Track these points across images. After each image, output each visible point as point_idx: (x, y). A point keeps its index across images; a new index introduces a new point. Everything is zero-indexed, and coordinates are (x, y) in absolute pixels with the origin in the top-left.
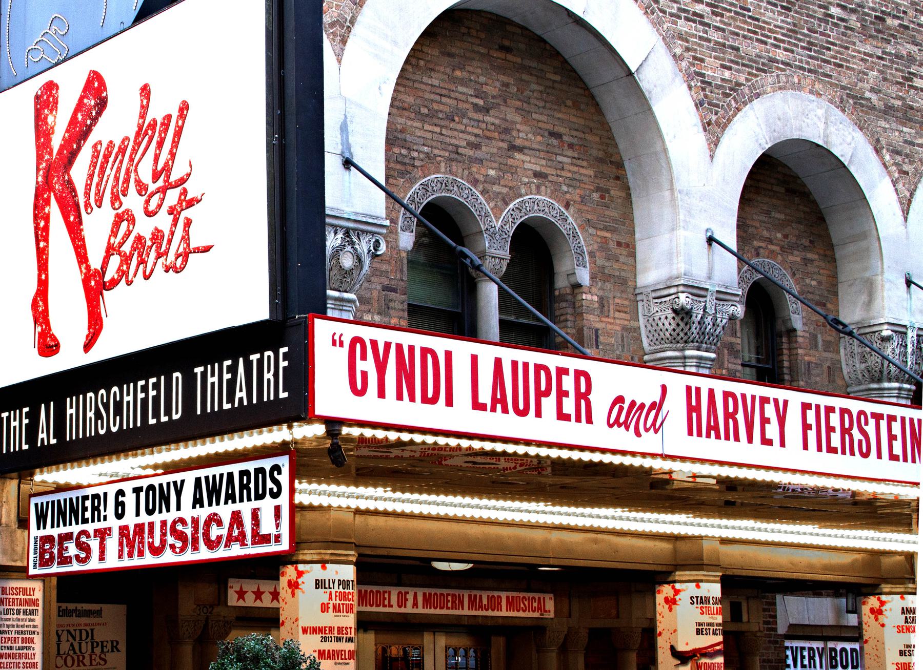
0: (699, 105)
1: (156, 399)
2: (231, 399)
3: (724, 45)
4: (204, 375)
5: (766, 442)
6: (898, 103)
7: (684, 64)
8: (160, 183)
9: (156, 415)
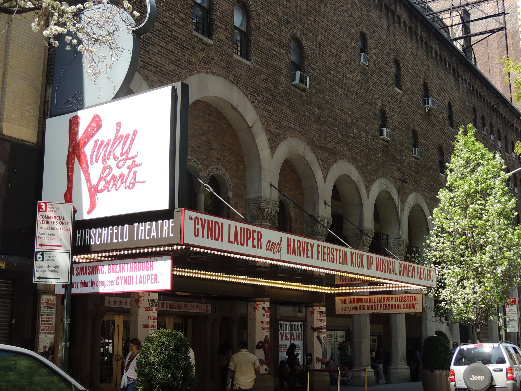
0: (269, 140)
1: (117, 234)
2: (149, 235)
4: (138, 227)
5: (308, 257)
6: (323, 145)
8: (124, 157)
9: (117, 238)
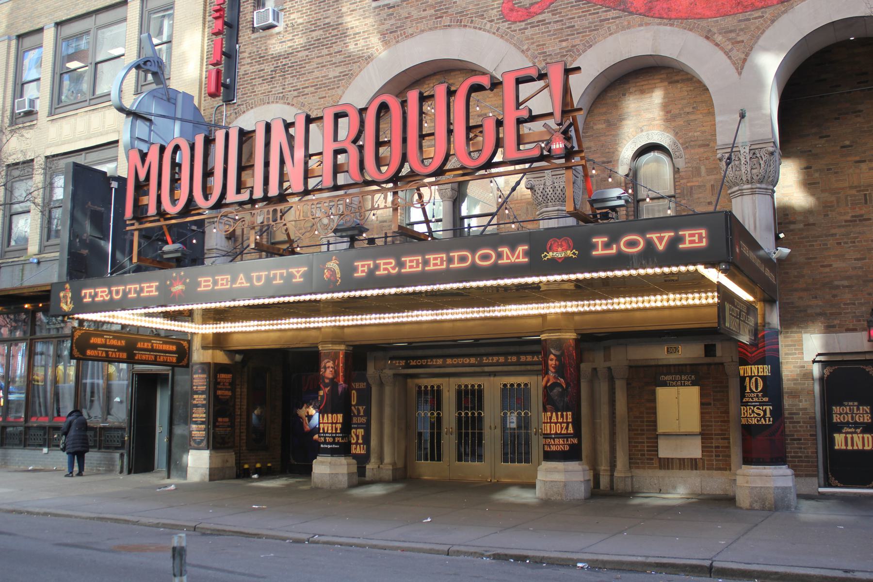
3: (562, 29)
7: (529, 53)
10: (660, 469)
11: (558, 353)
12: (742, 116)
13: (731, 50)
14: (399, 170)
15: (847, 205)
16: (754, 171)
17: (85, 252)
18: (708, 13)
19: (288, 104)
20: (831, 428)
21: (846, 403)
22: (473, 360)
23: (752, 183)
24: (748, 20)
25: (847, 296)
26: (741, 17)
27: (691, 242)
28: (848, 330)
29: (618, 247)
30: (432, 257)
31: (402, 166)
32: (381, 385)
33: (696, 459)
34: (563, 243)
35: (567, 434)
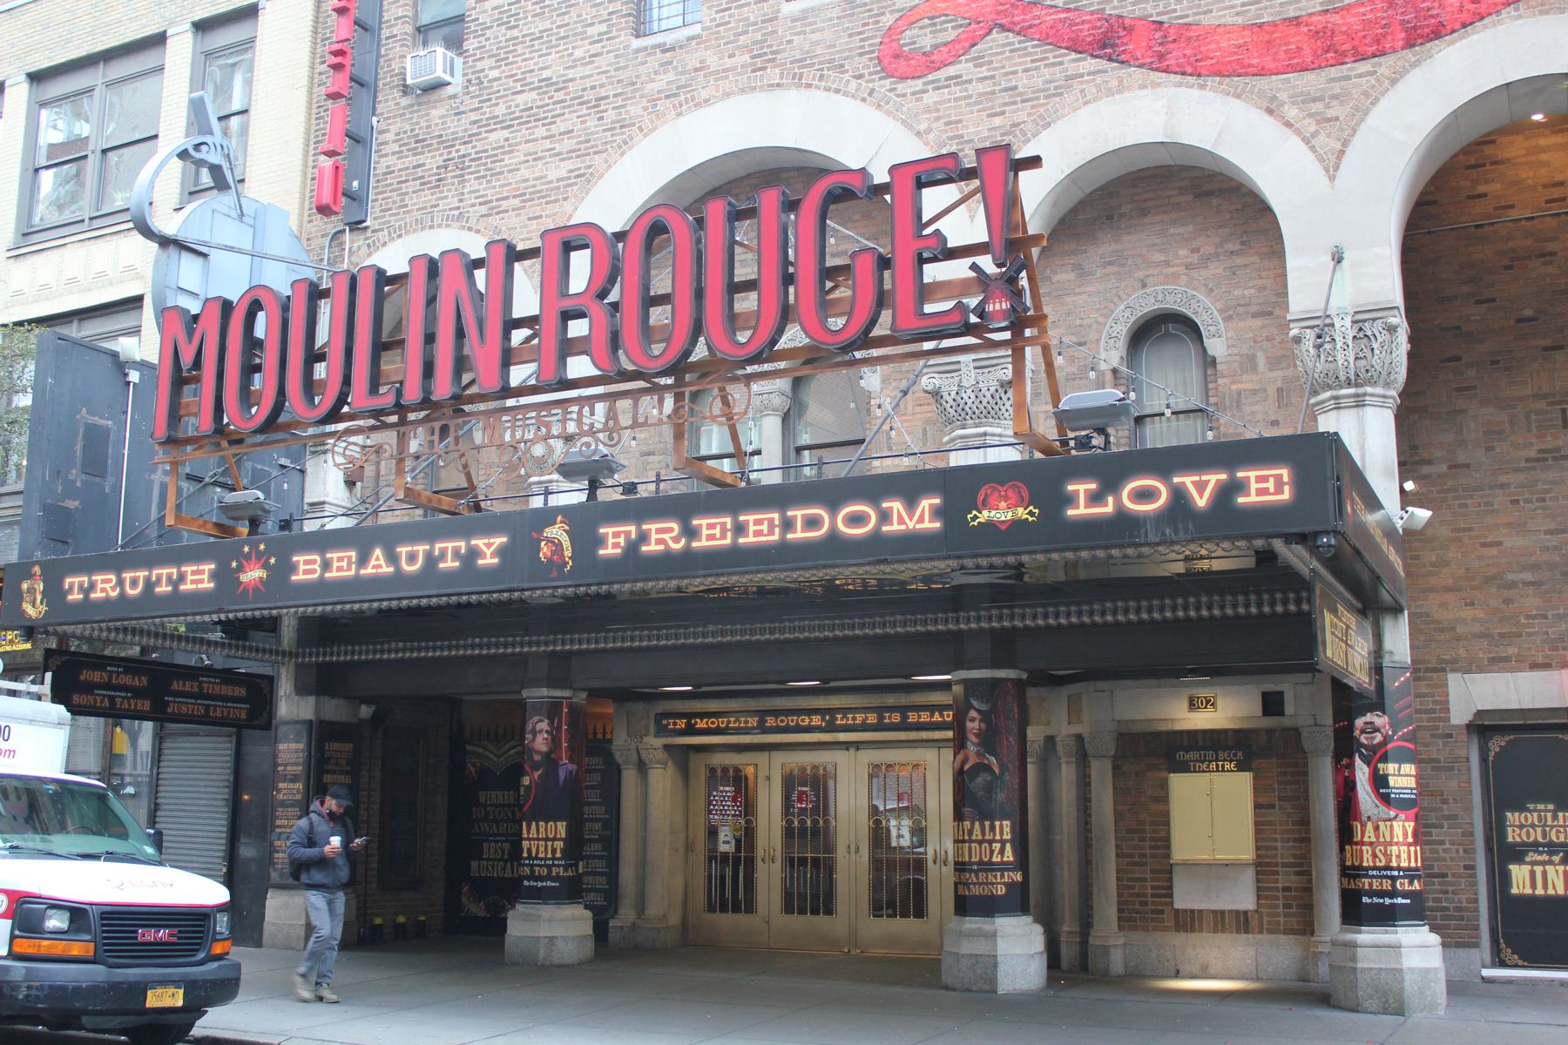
3: (993, 93)
7: (931, 136)
10: (1177, 930)
11: (984, 707)
12: (1338, 259)
13: (1315, 135)
14: (688, 353)
15: (1529, 430)
16: (1362, 363)
17: (72, 504)
18: (1271, 65)
19: (470, 229)
20: (1503, 854)
21: (1532, 806)
22: (816, 720)
23: (1357, 385)
24: (1348, 78)
25: (1532, 602)
26: (1334, 72)
27: (1260, 492)
28: (1534, 666)
29: (1118, 502)
30: (751, 518)
31: (694, 342)
32: (642, 767)
33: (1246, 913)
34: (1010, 493)
35: (1002, 863)
